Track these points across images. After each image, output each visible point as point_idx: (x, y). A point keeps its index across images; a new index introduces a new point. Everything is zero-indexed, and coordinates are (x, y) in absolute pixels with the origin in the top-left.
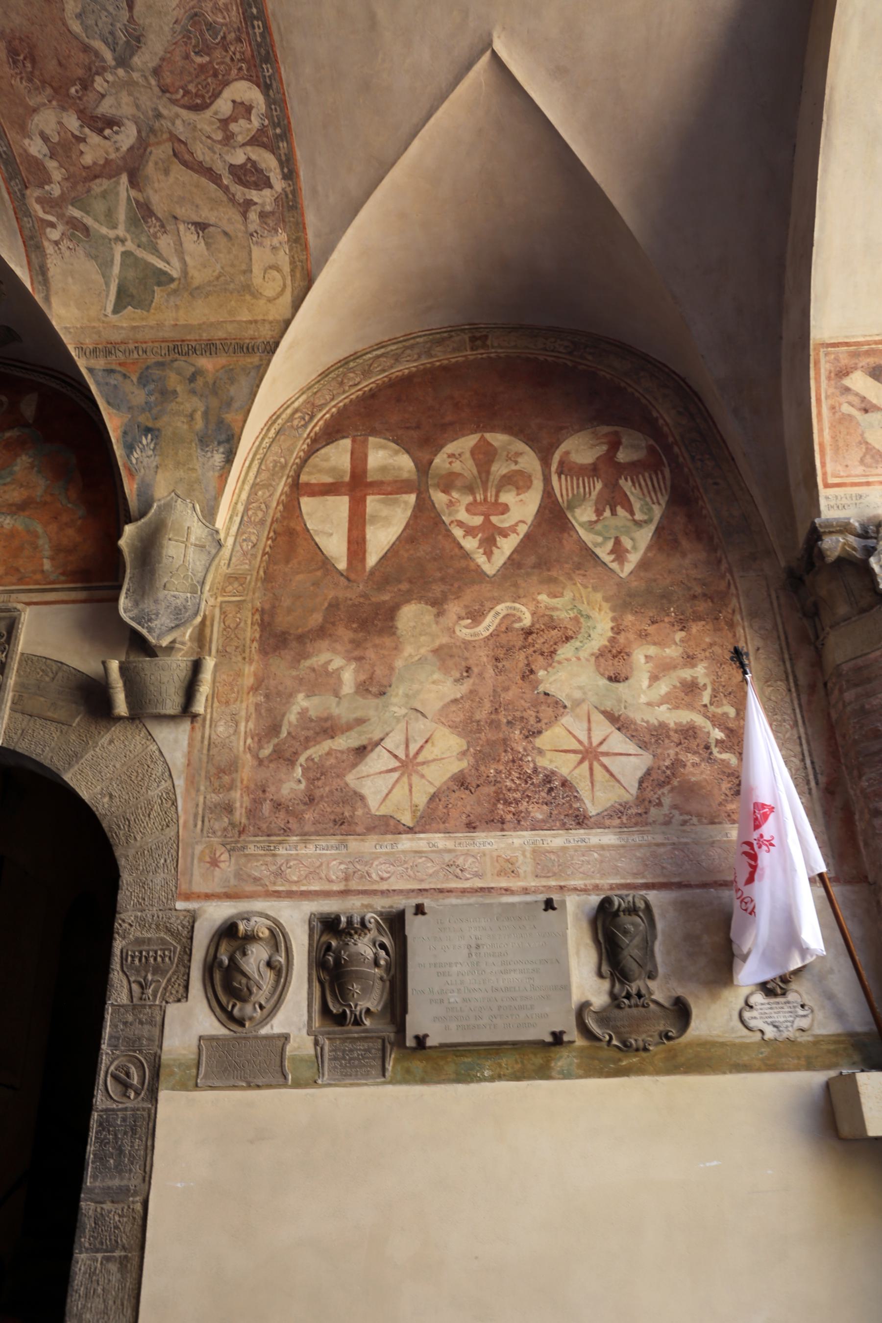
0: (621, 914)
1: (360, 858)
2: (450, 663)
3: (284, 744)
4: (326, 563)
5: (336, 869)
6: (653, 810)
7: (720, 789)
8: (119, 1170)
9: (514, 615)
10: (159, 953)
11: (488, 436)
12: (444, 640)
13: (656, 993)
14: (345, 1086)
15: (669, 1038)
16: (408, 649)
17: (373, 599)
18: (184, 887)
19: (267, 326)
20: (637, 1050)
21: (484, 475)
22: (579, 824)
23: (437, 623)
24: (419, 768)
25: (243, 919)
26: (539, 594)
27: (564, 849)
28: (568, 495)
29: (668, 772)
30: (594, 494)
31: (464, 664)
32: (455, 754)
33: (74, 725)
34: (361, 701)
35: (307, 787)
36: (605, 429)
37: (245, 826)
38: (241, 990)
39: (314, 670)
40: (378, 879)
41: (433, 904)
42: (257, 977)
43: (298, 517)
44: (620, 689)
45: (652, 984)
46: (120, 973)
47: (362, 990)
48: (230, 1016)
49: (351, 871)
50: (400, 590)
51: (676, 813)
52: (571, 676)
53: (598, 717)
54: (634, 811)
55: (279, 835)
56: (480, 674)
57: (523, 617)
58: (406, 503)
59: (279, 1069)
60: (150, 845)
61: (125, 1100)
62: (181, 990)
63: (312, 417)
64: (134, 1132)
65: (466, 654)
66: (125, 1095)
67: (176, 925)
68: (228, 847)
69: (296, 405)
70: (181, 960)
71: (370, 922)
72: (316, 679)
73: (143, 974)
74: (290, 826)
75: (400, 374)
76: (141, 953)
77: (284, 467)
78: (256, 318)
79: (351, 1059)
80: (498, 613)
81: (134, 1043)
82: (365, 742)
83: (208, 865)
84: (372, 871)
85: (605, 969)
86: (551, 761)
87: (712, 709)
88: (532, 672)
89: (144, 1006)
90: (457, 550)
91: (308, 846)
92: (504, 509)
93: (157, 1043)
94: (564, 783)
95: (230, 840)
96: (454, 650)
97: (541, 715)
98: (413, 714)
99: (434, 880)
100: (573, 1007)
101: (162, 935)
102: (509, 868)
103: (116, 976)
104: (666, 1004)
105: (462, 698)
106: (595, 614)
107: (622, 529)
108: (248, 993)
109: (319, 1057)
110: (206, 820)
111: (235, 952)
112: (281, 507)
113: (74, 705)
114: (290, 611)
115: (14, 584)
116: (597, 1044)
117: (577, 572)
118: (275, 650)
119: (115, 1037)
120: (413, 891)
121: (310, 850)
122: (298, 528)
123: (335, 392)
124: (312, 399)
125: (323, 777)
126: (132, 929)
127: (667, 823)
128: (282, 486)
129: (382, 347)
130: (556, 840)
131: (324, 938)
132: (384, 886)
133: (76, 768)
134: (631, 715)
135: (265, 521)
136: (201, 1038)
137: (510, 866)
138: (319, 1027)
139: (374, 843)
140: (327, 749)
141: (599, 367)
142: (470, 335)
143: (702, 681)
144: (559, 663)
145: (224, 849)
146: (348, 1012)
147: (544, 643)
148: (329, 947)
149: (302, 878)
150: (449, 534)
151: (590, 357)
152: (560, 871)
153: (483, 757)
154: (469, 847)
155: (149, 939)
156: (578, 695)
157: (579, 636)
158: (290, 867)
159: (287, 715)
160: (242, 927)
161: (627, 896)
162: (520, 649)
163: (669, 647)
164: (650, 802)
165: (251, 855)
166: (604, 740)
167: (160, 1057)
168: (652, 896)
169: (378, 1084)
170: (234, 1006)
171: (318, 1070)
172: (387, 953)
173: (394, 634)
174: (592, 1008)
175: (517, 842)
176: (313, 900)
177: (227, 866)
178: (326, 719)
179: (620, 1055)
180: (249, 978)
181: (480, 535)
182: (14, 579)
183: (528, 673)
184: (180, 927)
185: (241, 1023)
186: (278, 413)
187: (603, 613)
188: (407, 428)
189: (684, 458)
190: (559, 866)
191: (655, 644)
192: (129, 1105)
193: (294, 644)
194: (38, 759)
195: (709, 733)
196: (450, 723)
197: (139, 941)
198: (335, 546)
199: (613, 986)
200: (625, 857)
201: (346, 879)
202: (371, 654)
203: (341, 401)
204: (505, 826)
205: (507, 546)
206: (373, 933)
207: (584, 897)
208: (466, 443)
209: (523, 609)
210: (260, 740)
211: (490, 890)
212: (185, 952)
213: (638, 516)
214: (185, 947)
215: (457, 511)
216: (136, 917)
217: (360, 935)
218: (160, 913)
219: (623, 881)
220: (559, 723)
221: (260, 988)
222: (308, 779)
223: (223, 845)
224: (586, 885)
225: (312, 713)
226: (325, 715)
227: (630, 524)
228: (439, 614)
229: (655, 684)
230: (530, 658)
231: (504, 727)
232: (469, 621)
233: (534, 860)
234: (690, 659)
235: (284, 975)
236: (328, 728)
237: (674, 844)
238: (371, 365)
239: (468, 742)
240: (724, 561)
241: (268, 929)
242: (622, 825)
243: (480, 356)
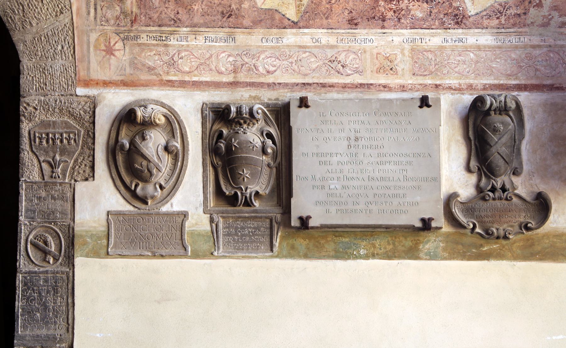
0: (492, 113)
1: (247, 52)
5: (225, 62)
6: (532, 11)
8: (45, 321)
10: (65, 135)
13: (520, 188)
14: (238, 258)
15: (528, 229)
18: (82, 74)
20: (498, 238)
22: (457, 23)
25: (141, 106)
27: (441, 48)
37: (136, 15)
38: (142, 171)
40: (264, 72)
41: (316, 98)
42: (156, 160)
45: (515, 179)
46: (30, 153)
47: (251, 174)
48: (134, 194)
49: (239, 64)
51: (555, 14)
54: (513, 11)
59: (180, 242)
60: (46, 31)
61: (45, 264)
62: (88, 170)
64: (56, 292)
66: (45, 260)
67: (78, 109)
68: (122, 35)
70: (85, 143)
71: (258, 113)
73: (51, 154)
74: (179, 16)
76: (47, 135)
79: (242, 235)
81: (48, 217)
83: (104, 53)
84: (259, 64)
85: (474, 164)
89: (55, 184)
93: (69, 216)
95: (123, 29)
99: (317, 75)
100: (442, 197)
101: (66, 119)
102: (388, 66)
103: (26, 156)
104: (528, 199)
108: (149, 174)
109: (215, 232)
110: (99, 8)
111: (135, 137)
116: (462, 231)
119: (31, 210)
120: (297, 85)
121: (201, 41)
126: (38, 112)
127: (545, 25)
130: (434, 39)
131: (216, 127)
132: (270, 79)
136: (108, 213)
137: (389, 63)
138: (213, 206)
139: (261, 37)
145: (118, 38)
146: (239, 194)
148: (221, 135)
149: (193, 69)
152: (437, 70)
154: (350, 44)
155: (54, 122)
158: (182, 58)
160: (140, 113)
161: (500, 95)
165: (144, 44)
167: (73, 229)
168: (523, 97)
169: (266, 257)
170: (136, 186)
171: (214, 243)
172: (274, 143)
174: (459, 199)
175: (395, 40)
176: (205, 91)
177: (122, 55)
179: (482, 241)
180: (149, 161)
184: (82, 112)
185: (144, 200)
190: (435, 65)
192: (49, 269)
197: (44, 124)
199: (479, 180)
200: (500, 58)
201: (235, 71)
204: (385, 24)
206: (261, 124)
207: (457, 96)
211: (369, 85)
212: (88, 134)
214: (88, 131)
216: (40, 101)
217: (249, 125)
218: (62, 98)
219: (496, 82)
221: (159, 170)
223: (117, 34)
224: (460, 85)
233: (412, 58)
235: (180, 159)
237: (550, 46)
241: (164, 116)
242: (500, 26)
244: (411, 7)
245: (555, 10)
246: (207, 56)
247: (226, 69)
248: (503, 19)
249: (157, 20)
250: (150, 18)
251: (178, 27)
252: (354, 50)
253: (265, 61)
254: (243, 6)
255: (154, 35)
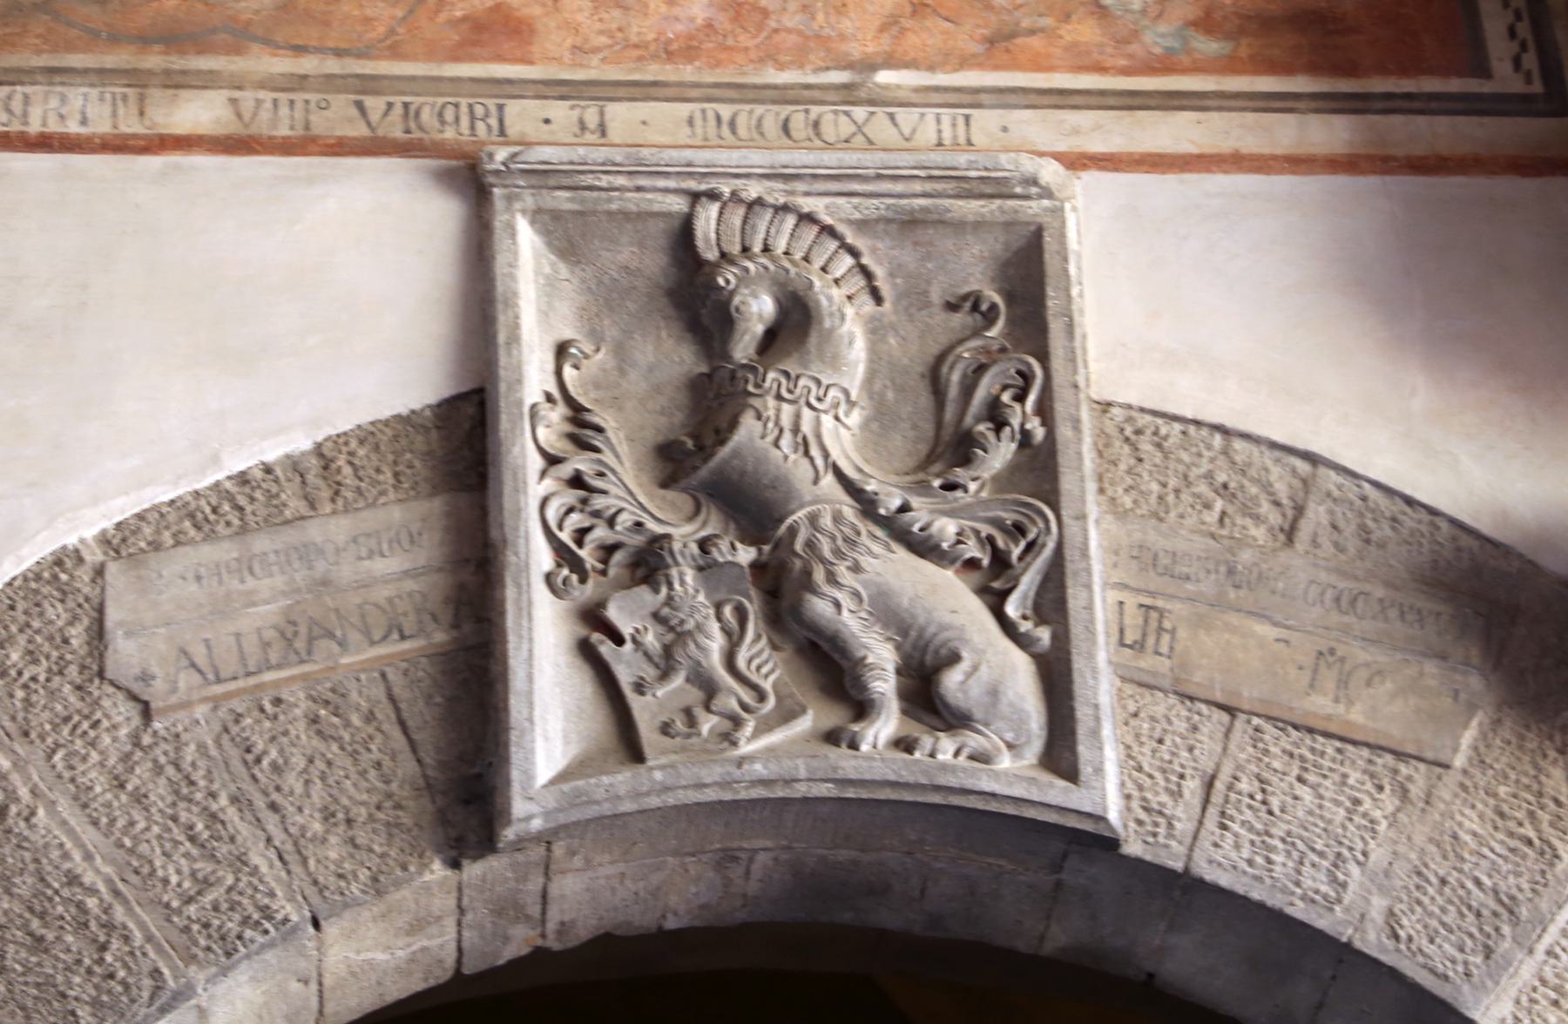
33: (1459, 761)
113: (1431, 667)
115: (964, 63)
133: (1527, 970)
182: (967, 38)
194: (1322, 923)
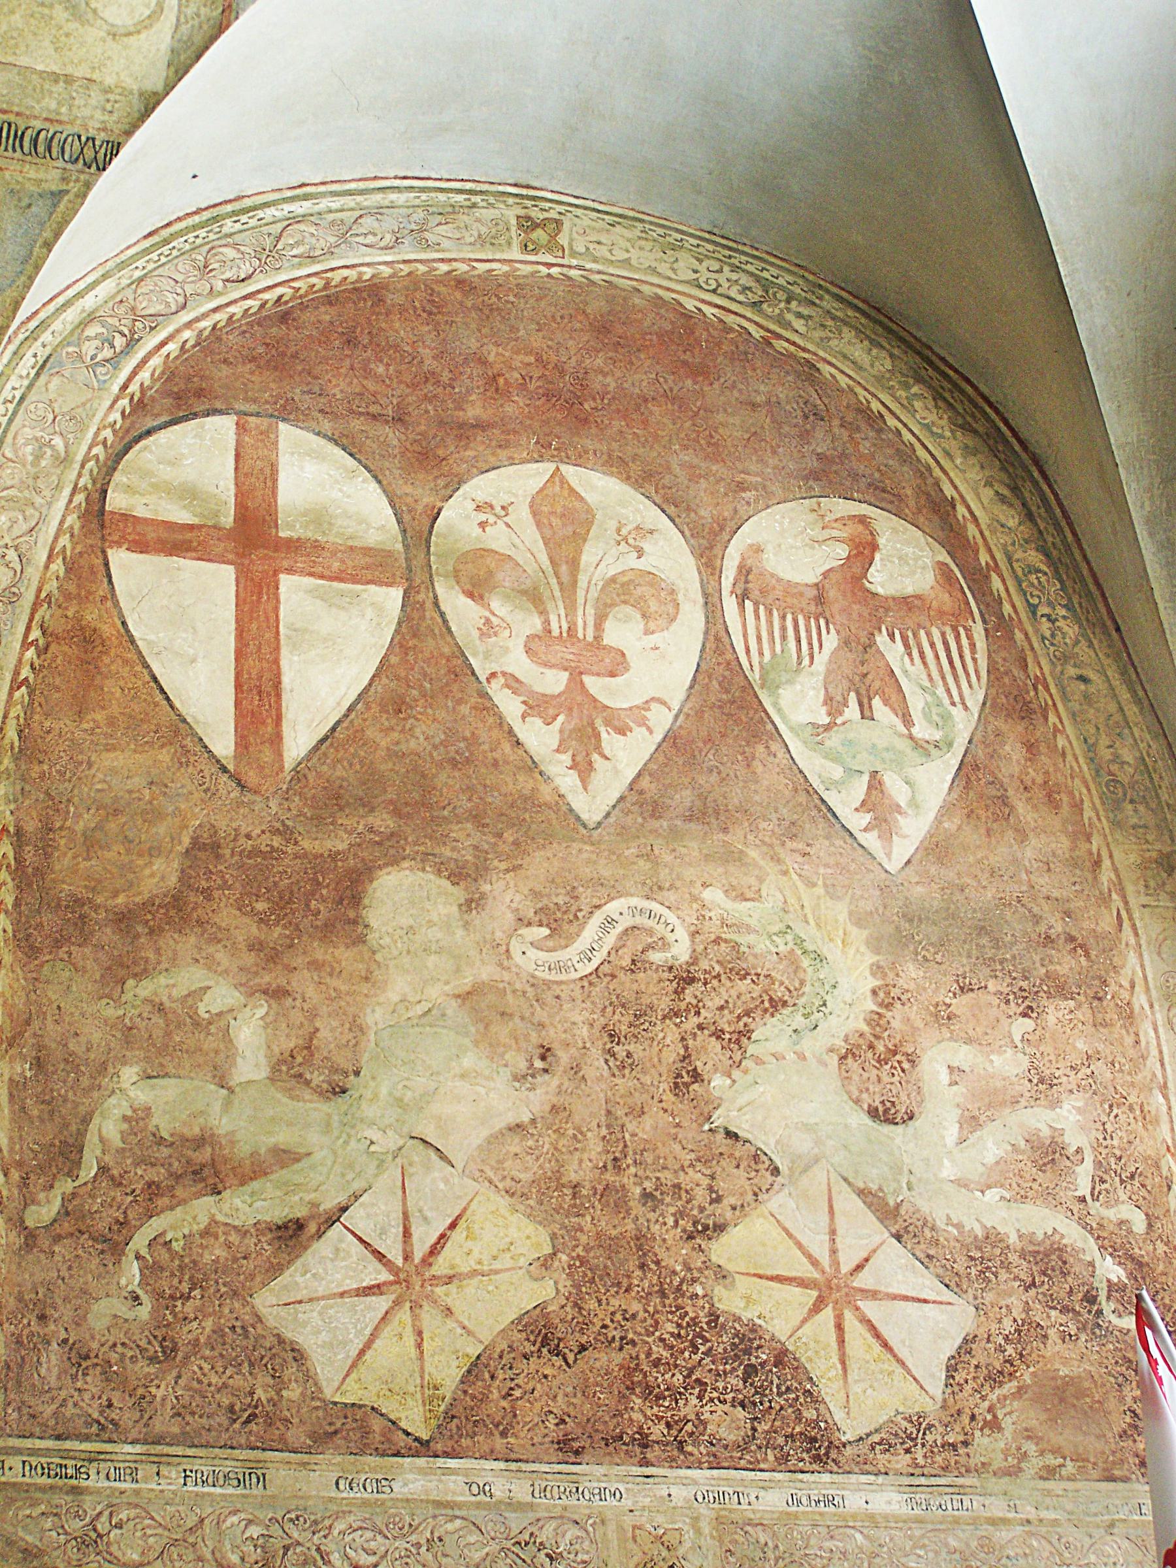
2: (502, 1031)
3: (93, 1197)
4: (179, 733)
6: (981, 1440)
7: (1122, 1399)
9: (650, 932)
11: (568, 470)
12: (486, 972)
16: (398, 986)
17: (306, 844)
19: (96, 97)
21: (564, 569)
22: (817, 1458)
23: (466, 925)
24: (440, 1290)
26: (705, 885)
28: (761, 654)
29: (1010, 1350)
30: (822, 659)
31: (534, 1038)
32: (523, 1262)
34: (282, 1104)
35: (154, 1310)
36: (843, 507)
39: (160, 1008)
43: (104, 599)
44: (898, 1141)
49: (277, 1544)
50: (371, 830)
51: (1030, 1447)
52: (782, 1094)
53: (849, 1204)
55: (87, 1438)
56: (575, 1069)
57: (671, 937)
58: (379, 609)
63: (132, 343)
65: (541, 1014)
69: (89, 302)
72: (168, 1034)
75: (352, 274)
77: (64, 461)
78: (69, 70)
80: (611, 921)
82: (300, 1213)
84: (329, 1546)
86: (748, 1299)
87: (1095, 1207)
88: (696, 1076)
90: (507, 747)
91: (164, 1470)
92: (617, 665)
94: (781, 1357)
96: (510, 997)
97: (721, 1185)
98: (418, 1153)
105: (533, 1121)
106: (833, 952)
107: (885, 755)
112: (58, 567)
114: (91, 844)
117: (790, 844)
118: (57, 944)
122: (106, 630)
123: (189, 290)
124: (129, 293)
125: (196, 1293)
128: (58, 512)
129: (306, 197)
130: (770, 1494)
134: (925, 1208)
135: (19, 596)
137: (665, 1553)
140: (204, 1221)
141: (821, 353)
142: (522, 212)
143: (1074, 1140)
144: (759, 1061)
147: (721, 1008)
149: (153, 1555)
150: (486, 706)
151: (799, 324)
153: (588, 1275)
156: (803, 1144)
157: (801, 1001)
158: (119, 1526)
159: (96, 1120)
162: (664, 1017)
163: (1000, 1051)
164: (973, 1417)
166: (867, 1260)
173: (361, 940)
178: (200, 1142)
181: (561, 718)
183: (686, 1079)
186: (42, 315)
187: (851, 951)
188: (374, 417)
189: (1014, 606)
190: (777, 1560)
191: (969, 1041)
193: (107, 935)
195: (1092, 1264)
196: (508, 1183)
198: (206, 695)
200: (924, 1546)
202: (304, 983)
203: (205, 316)
205: (627, 756)
208: (516, 482)
209: (671, 917)
210: (25, 1181)
213: (921, 730)
215: (506, 650)
220: (762, 1209)
222: (159, 1295)
225: (162, 1123)
226: (197, 1130)
227: (904, 745)
228: (472, 904)
229: (973, 1138)
230: (691, 1042)
231: (637, 1209)
232: (545, 931)
233: (721, 1541)
234: (1044, 1084)
236: (205, 1167)
238: (278, 238)
239: (553, 1237)
240: (1106, 863)
243: (544, 270)
244: (707, 1416)
245: (1029, 1438)
246: (190, 1524)
247: (243, 1559)
248: (919, 1453)
249: (52, 1422)
250: (34, 1417)
251: (110, 1441)
252: (576, 1517)
253: (348, 1539)
254: (285, 1393)
255: (43, 1460)
